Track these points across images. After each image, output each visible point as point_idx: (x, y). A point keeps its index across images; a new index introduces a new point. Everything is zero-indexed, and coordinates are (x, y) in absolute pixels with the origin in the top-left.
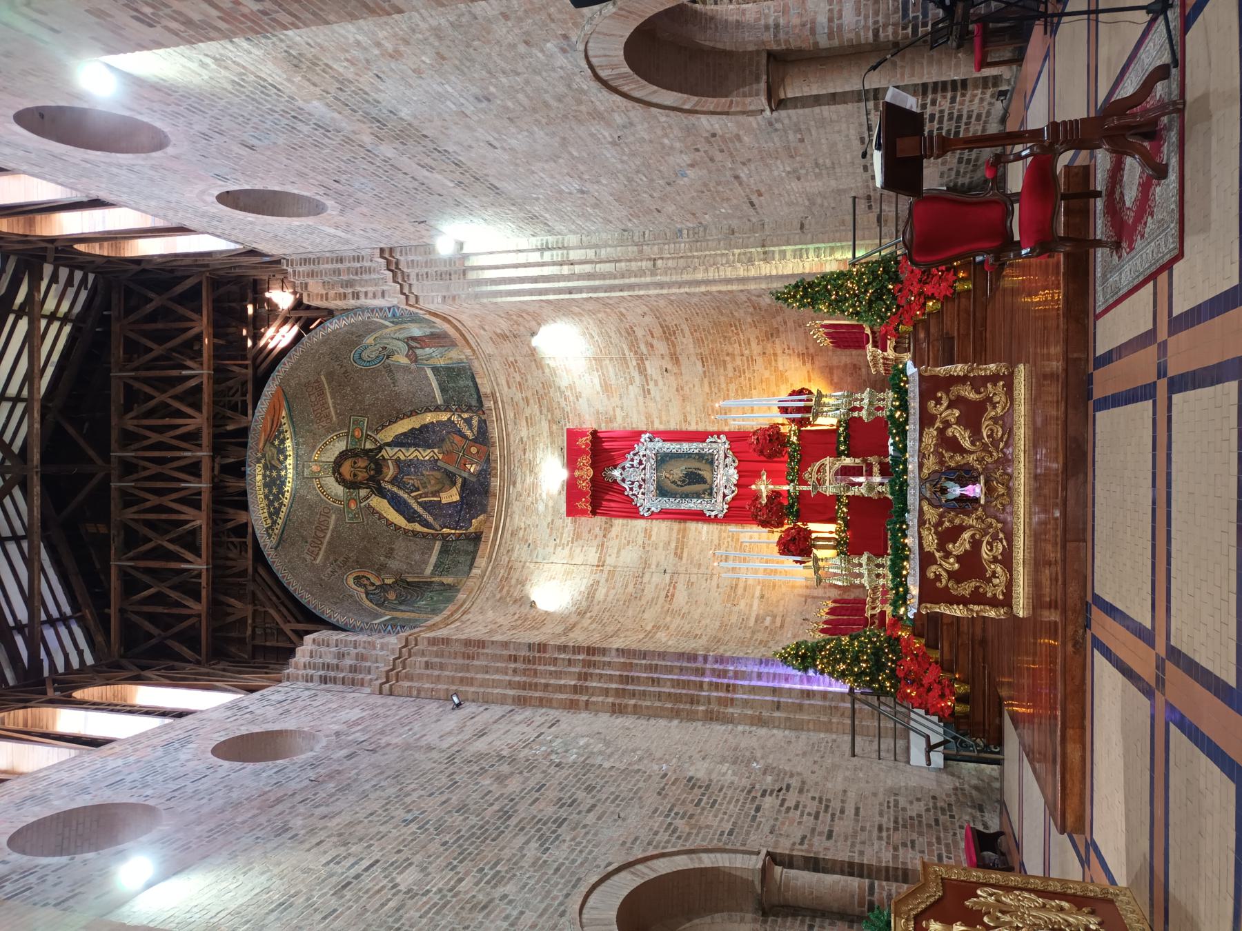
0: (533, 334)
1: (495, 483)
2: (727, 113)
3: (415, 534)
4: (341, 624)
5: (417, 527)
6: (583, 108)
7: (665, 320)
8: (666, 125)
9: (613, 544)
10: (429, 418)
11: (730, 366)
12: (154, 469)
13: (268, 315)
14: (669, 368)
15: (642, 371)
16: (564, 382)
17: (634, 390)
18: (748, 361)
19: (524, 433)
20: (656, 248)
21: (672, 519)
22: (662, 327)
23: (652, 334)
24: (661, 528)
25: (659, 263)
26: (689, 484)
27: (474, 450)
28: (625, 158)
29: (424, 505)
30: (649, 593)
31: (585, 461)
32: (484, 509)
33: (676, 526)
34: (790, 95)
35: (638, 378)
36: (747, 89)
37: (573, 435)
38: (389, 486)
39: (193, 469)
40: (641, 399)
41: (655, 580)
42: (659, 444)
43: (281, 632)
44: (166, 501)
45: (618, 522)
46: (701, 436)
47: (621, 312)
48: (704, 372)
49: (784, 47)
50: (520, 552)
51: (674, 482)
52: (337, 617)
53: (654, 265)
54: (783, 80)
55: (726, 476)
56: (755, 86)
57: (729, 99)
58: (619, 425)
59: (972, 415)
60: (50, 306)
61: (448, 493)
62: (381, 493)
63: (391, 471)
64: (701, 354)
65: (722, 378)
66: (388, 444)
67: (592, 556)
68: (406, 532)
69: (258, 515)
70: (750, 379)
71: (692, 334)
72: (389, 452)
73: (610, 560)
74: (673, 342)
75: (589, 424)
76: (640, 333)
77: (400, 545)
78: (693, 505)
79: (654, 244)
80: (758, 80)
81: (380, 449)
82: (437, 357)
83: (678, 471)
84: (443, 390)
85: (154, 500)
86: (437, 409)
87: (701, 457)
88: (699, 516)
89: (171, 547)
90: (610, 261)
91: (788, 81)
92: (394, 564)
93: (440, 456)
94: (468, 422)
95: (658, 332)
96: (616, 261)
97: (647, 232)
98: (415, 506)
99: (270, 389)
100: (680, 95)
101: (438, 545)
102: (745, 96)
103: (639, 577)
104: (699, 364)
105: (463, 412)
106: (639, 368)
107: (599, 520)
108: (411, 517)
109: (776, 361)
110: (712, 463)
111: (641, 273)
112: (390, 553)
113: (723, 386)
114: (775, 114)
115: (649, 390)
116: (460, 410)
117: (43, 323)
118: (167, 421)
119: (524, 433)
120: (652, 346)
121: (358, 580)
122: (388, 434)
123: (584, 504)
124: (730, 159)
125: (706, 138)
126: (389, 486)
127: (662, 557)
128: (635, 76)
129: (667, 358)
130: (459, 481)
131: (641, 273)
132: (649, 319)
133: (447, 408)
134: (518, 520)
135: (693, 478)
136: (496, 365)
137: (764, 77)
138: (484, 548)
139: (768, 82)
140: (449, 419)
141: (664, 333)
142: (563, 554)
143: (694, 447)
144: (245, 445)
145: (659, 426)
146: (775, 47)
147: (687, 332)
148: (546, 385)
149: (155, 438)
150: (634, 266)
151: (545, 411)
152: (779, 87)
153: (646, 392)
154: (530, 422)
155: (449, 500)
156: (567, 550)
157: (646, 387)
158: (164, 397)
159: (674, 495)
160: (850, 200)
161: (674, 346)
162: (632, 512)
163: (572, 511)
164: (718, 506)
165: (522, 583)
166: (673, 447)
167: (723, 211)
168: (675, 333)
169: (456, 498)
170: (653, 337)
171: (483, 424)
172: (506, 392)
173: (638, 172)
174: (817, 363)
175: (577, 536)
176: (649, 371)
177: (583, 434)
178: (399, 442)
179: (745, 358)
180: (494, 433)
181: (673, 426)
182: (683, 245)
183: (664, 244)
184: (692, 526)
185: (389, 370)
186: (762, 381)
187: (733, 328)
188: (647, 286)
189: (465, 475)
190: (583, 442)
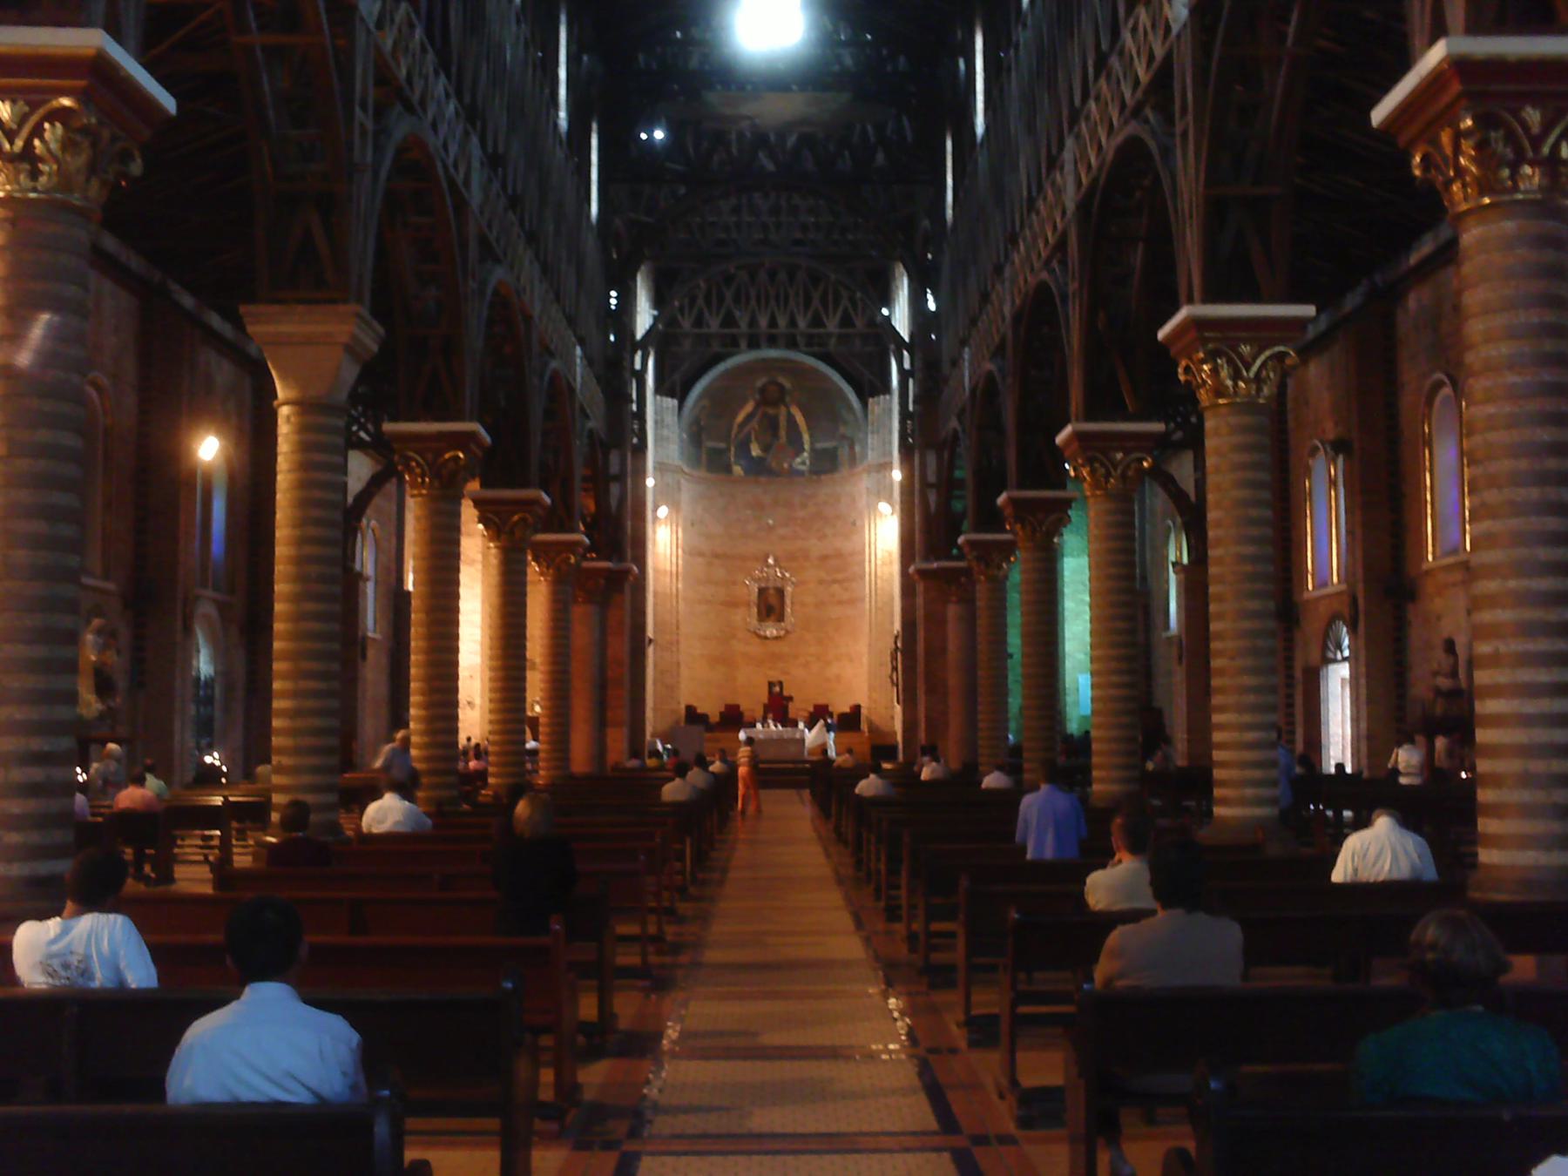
1: (763, 479)
63: (771, 411)
82: (843, 453)
83: (773, 600)
85: (753, 293)
94: (803, 463)
101: (722, 445)
133: (813, 450)
158: (816, 303)
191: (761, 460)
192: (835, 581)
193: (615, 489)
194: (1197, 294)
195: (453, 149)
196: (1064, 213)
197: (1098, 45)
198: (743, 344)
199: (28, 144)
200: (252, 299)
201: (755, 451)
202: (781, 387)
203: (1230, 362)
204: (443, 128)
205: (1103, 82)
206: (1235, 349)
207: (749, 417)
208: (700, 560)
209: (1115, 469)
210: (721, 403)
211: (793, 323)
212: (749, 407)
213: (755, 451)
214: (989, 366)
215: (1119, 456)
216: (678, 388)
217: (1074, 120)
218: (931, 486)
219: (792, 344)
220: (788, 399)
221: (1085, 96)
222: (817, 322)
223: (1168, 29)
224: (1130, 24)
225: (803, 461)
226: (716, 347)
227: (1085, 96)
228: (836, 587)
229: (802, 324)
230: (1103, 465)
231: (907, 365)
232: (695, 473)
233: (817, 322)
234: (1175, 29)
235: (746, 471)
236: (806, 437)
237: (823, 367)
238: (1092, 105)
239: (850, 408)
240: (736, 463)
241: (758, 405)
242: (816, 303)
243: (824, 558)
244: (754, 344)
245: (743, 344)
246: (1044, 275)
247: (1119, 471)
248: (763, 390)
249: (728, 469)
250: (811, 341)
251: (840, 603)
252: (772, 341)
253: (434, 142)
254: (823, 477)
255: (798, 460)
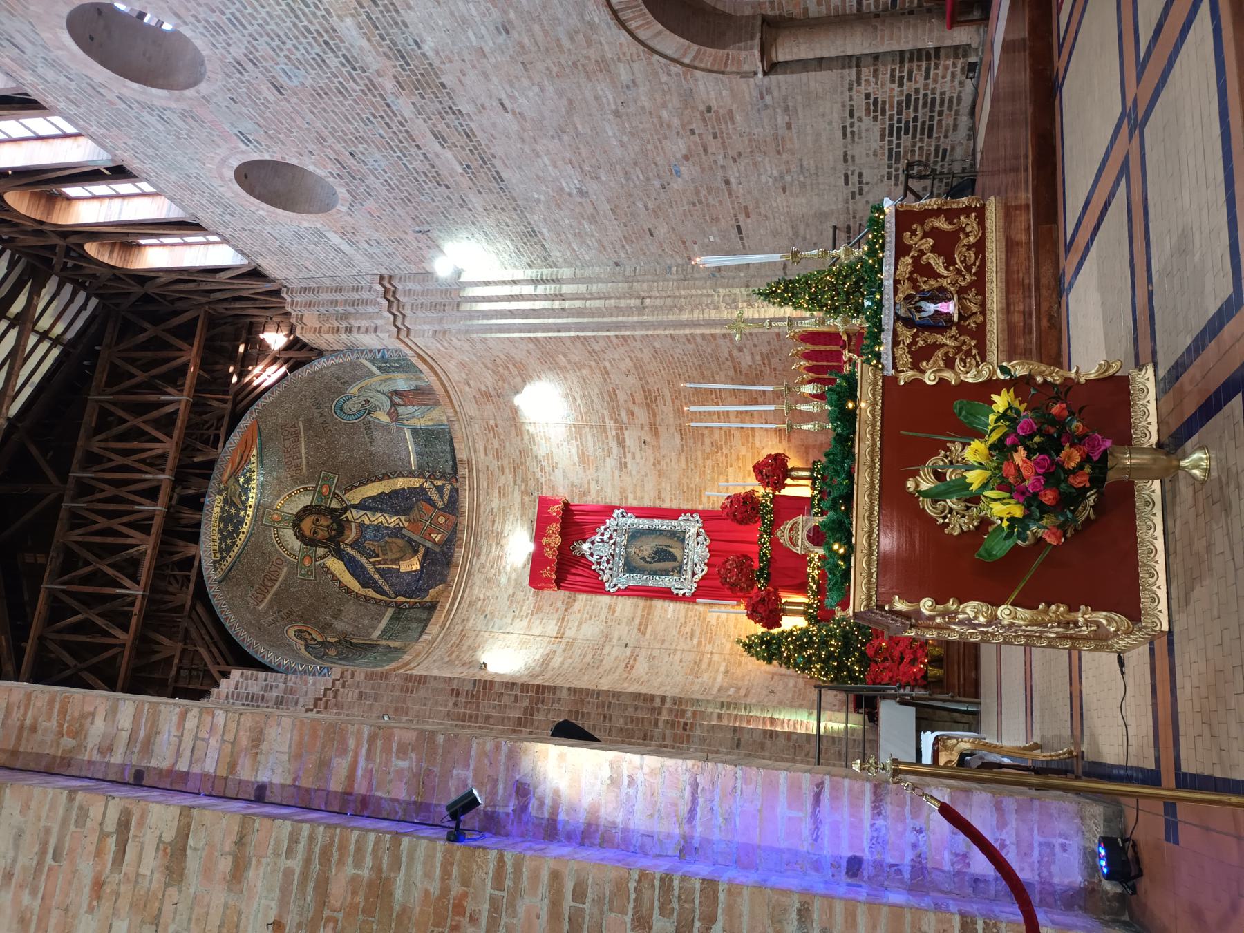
0: (517, 392)
1: (459, 553)
2: (723, 73)
3: (367, 599)
4: (273, 665)
5: (371, 593)
6: (592, 53)
7: (647, 383)
8: (666, 88)
9: (574, 618)
10: (401, 483)
11: (707, 441)
12: (110, 491)
13: (260, 352)
14: (648, 440)
15: (621, 442)
16: (541, 451)
17: (611, 462)
18: (726, 435)
19: (495, 504)
20: (645, 285)
21: (638, 596)
22: (644, 391)
23: (634, 400)
24: (627, 606)
25: (647, 301)
26: (659, 561)
27: (442, 520)
28: (625, 139)
29: (380, 572)
30: (608, 663)
31: (554, 528)
32: (443, 580)
33: (641, 603)
34: (781, 58)
35: (615, 450)
36: (742, 44)
37: (544, 503)
38: (348, 549)
39: (152, 494)
40: (617, 472)
41: (614, 653)
42: (632, 521)
44: (115, 524)
45: (582, 598)
46: (673, 514)
47: (605, 368)
48: (682, 445)
49: (777, 13)
50: (476, 621)
51: (643, 559)
53: (642, 303)
54: (775, 40)
55: (696, 551)
56: (749, 43)
57: (726, 51)
58: (592, 499)
59: (945, 244)
60: (44, 324)
61: (408, 562)
62: (340, 555)
63: (352, 534)
64: (680, 425)
65: (699, 454)
66: (355, 506)
67: (552, 628)
68: (358, 596)
69: (208, 548)
70: (726, 455)
71: (673, 402)
72: (353, 515)
73: (570, 633)
74: (653, 410)
75: (563, 493)
76: (622, 397)
77: (350, 609)
78: (663, 582)
79: (643, 281)
80: (752, 38)
81: (345, 510)
83: (647, 548)
85: (103, 523)
86: (411, 474)
87: (672, 534)
88: (666, 594)
89: (110, 571)
90: (600, 298)
91: (779, 41)
92: (340, 625)
93: (406, 524)
94: (440, 490)
95: (639, 397)
96: (606, 298)
97: (638, 268)
98: (372, 572)
99: (247, 421)
100: (682, 40)
102: (740, 49)
103: (599, 649)
104: (678, 436)
105: (436, 479)
106: (618, 438)
107: (562, 595)
108: (366, 582)
109: (753, 436)
110: (683, 540)
111: (629, 310)
112: (338, 614)
113: (700, 462)
114: (767, 79)
115: (625, 463)
116: (433, 476)
117: (33, 339)
118: (135, 445)
119: (495, 504)
120: (633, 414)
121: (299, 633)
122: (356, 496)
123: (549, 573)
124: (722, 151)
125: (702, 113)
126: (348, 549)
127: (622, 632)
128: (643, 6)
129: (646, 428)
130: (422, 550)
131: (629, 310)
132: (632, 380)
133: (421, 474)
134: (477, 591)
135: (663, 555)
136: (476, 429)
137: (759, 35)
138: (439, 617)
139: (761, 38)
140: (421, 486)
141: (646, 399)
142: (520, 625)
143: (666, 524)
144: (208, 477)
145: (632, 502)
146: (770, 13)
147: (668, 399)
148: (524, 453)
149: (119, 460)
150: (623, 303)
151: (519, 481)
152: (771, 45)
153: (623, 465)
154: (503, 493)
155: (409, 569)
156: (525, 622)
157: (623, 460)
159: (642, 571)
160: (831, 231)
161: (654, 415)
162: (597, 588)
163: (536, 581)
164: (685, 586)
165: (473, 649)
166: (645, 523)
167: (712, 239)
168: (656, 400)
169: (416, 567)
170: (634, 403)
171: (455, 491)
172: (482, 459)
173: (635, 164)
174: (793, 440)
175: (537, 609)
176: (627, 443)
177: (556, 502)
178: (365, 506)
179: (723, 432)
180: (465, 502)
181: (647, 502)
182: (671, 283)
183: (653, 281)
184: (659, 604)
185: (368, 426)
186: (738, 458)
187: (713, 396)
188: (633, 326)
189: (429, 545)
190: (554, 510)
191: (428, 557)
207: (354, 568)
255: (434, 494)
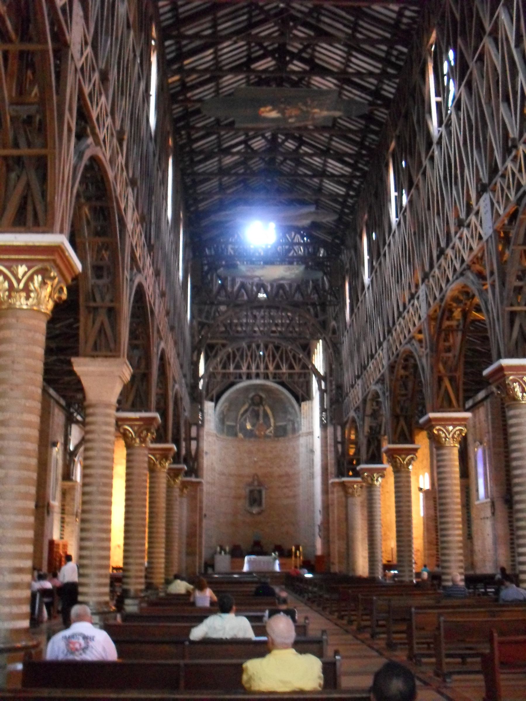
1: (252, 439)
39: (258, 367)
43: (213, 390)
52: (218, 408)
63: (256, 408)
82: (289, 427)
83: (256, 495)
84: (281, 426)
85: (249, 354)
86: (275, 423)
94: (271, 432)
158: (278, 358)
192: (286, 487)
193: (194, 444)
194: (502, 354)
195: (151, 288)
196: (420, 318)
197: (439, 244)
198: (244, 377)
199: (26, 286)
200: (77, 354)
201: (249, 427)
202: (261, 398)
203: (520, 385)
204: (148, 280)
205: (442, 260)
206: (522, 379)
207: (246, 411)
208: (223, 477)
209: (449, 434)
210: (233, 404)
211: (267, 368)
212: (246, 407)
213: (249, 427)
214: (373, 387)
215: (451, 428)
216: (214, 399)
217: (425, 277)
218: (339, 443)
219: (266, 377)
220: (264, 403)
221: (431, 267)
222: (278, 367)
223: (480, 238)
224: (458, 235)
225: (270, 431)
226: (232, 379)
227: (431, 267)
228: (285, 490)
229: (271, 368)
230: (444, 432)
231: (323, 387)
232: (221, 437)
233: (278, 367)
234: (485, 238)
235: (245, 436)
236: (272, 420)
237: (280, 388)
238: (436, 271)
239: (293, 407)
240: (240, 432)
241: (250, 406)
242: (278, 358)
243: (280, 476)
244: (249, 377)
245: (244, 377)
246: (409, 346)
247: (451, 435)
248: (252, 399)
249: (236, 435)
250: (275, 376)
251: (288, 497)
252: (257, 376)
253: (146, 286)
254: (280, 438)
255: (268, 431)
